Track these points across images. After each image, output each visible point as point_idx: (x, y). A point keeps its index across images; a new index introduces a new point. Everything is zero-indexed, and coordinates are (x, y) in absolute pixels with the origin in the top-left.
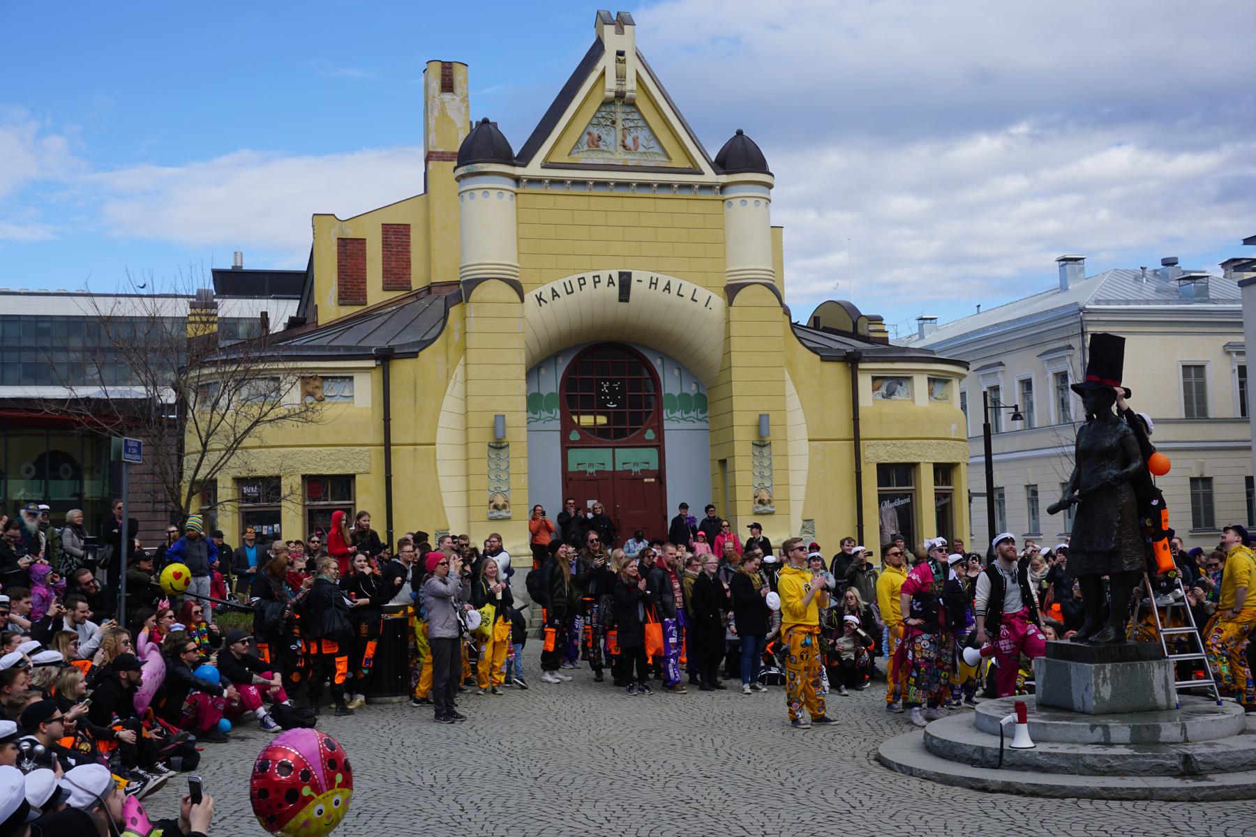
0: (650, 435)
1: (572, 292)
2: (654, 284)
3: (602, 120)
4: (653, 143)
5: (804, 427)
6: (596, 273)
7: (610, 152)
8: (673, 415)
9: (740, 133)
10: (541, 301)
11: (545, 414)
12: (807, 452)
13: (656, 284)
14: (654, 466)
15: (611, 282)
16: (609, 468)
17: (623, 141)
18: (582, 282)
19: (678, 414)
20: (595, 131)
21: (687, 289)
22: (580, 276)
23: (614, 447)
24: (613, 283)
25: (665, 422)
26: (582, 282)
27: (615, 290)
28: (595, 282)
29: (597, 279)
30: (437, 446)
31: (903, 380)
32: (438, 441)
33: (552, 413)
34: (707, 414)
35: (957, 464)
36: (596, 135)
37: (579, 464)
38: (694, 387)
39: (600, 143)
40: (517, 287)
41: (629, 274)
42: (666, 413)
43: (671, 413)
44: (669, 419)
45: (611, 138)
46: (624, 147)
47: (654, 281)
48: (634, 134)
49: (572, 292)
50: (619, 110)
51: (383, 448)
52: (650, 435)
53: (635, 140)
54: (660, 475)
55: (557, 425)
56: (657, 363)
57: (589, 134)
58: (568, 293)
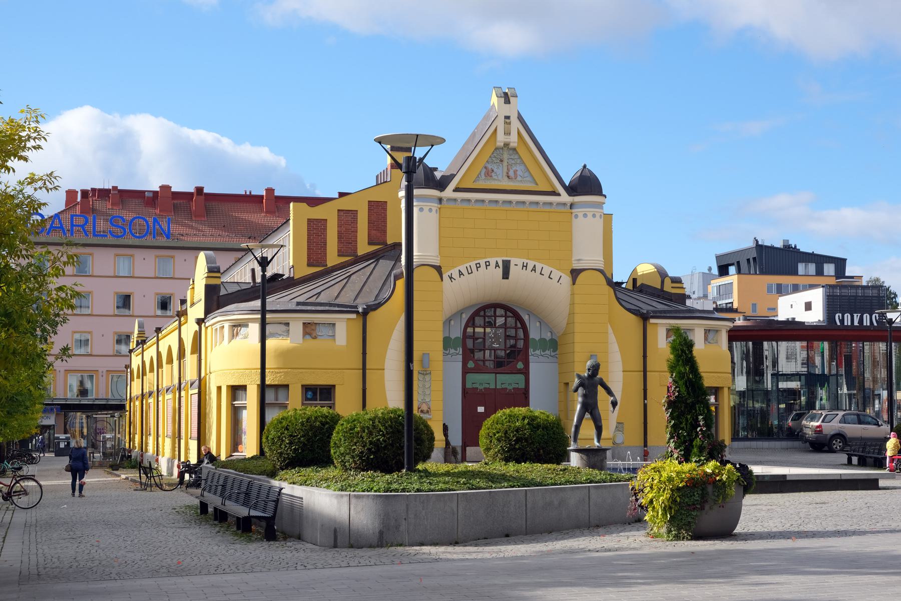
0: (520, 365)
1: (472, 272)
2: (525, 266)
3: (494, 159)
4: (527, 174)
5: (620, 364)
6: (487, 260)
7: (499, 180)
8: (534, 353)
9: (585, 166)
10: (452, 279)
11: (452, 351)
12: (621, 379)
13: (526, 267)
14: (522, 385)
15: (497, 265)
16: (492, 386)
17: (508, 173)
18: (478, 266)
19: (538, 352)
21: (547, 270)
23: (496, 373)
24: (498, 266)
25: (530, 357)
26: (478, 266)
27: (500, 271)
28: (487, 266)
29: (488, 264)
30: (385, 370)
32: (385, 368)
33: (457, 350)
34: (557, 352)
35: (722, 388)
36: (490, 169)
37: (473, 383)
38: (549, 334)
39: (493, 174)
40: (438, 269)
41: (509, 261)
42: (531, 351)
43: (533, 351)
44: (532, 355)
46: (508, 177)
47: (525, 265)
48: (514, 168)
49: (472, 272)
50: (505, 153)
51: (362, 371)
52: (520, 365)
53: (515, 172)
56: (526, 318)
57: (486, 168)
58: (469, 274)
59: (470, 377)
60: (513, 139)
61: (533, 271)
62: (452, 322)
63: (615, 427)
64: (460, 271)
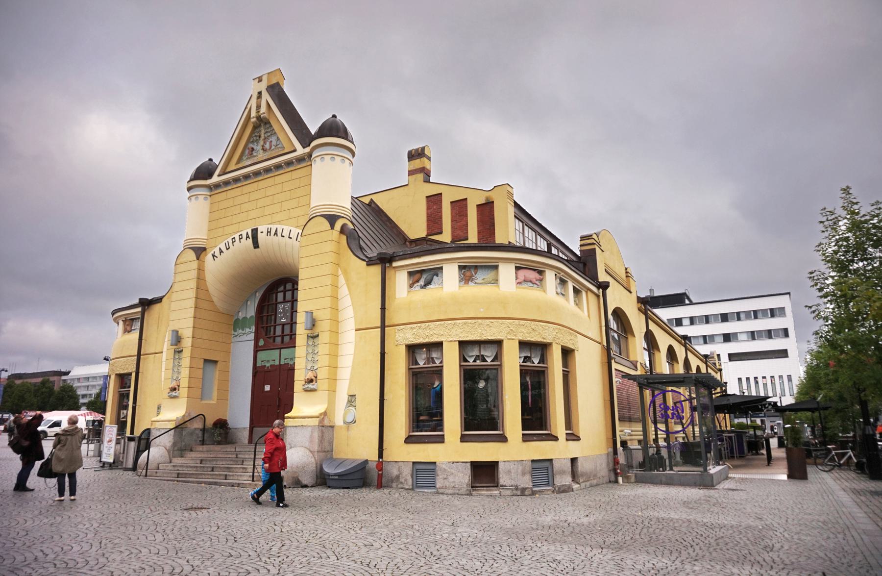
2: (269, 232)
5: (352, 320)
11: (248, 330)
13: (270, 232)
15: (248, 237)
16: (277, 363)
20: (251, 145)
22: (232, 237)
27: (250, 241)
31: (437, 271)
37: (262, 361)
55: (252, 336)
59: (262, 355)
60: (263, 109)
62: (249, 303)
63: (346, 401)
64: (220, 249)
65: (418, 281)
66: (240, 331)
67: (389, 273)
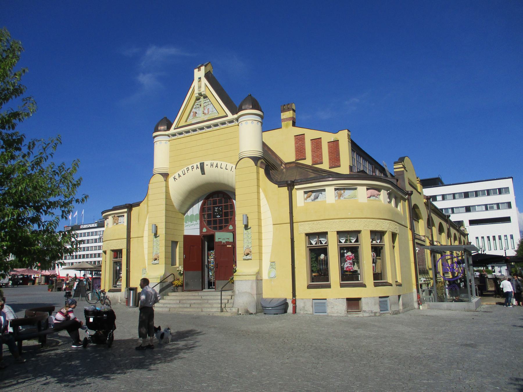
2: (212, 165)
3: (197, 106)
11: (195, 222)
13: (213, 165)
15: (197, 168)
17: (203, 111)
18: (188, 169)
22: (187, 167)
24: (198, 168)
26: (188, 169)
41: (204, 162)
45: (200, 111)
46: (204, 113)
54: (234, 244)
55: (198, 226)
61: (217, 167)
64: (179, 174)
65: (310, 197)
66: (190, 223)
67: (294, 191)
